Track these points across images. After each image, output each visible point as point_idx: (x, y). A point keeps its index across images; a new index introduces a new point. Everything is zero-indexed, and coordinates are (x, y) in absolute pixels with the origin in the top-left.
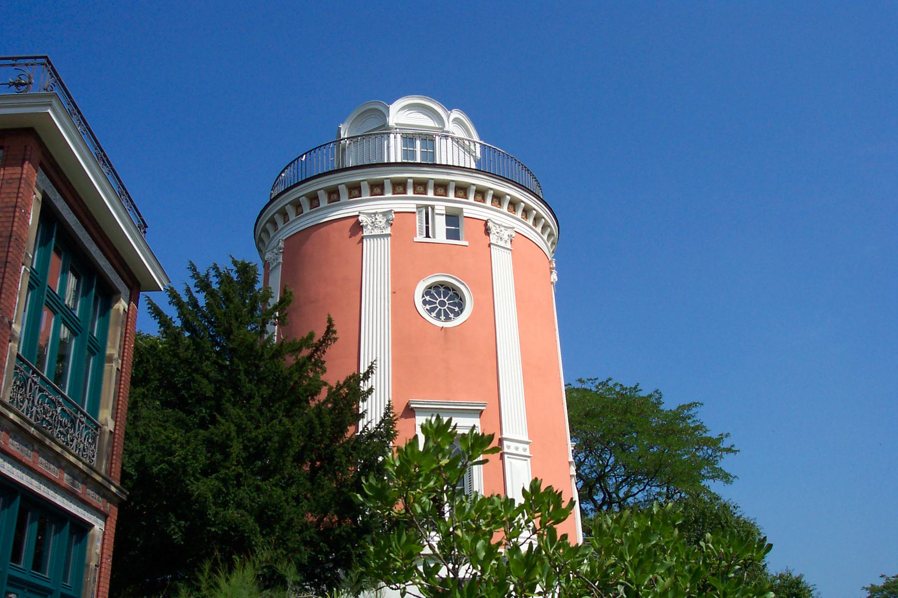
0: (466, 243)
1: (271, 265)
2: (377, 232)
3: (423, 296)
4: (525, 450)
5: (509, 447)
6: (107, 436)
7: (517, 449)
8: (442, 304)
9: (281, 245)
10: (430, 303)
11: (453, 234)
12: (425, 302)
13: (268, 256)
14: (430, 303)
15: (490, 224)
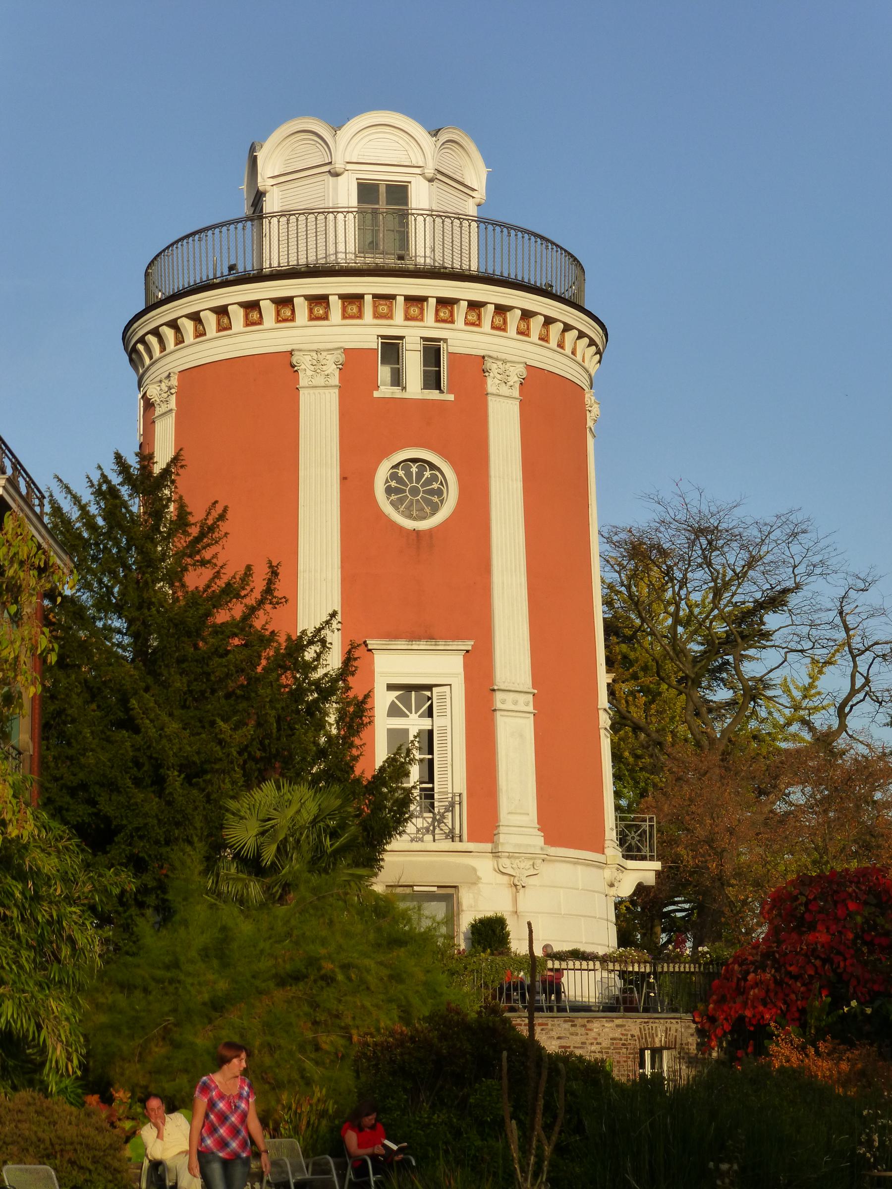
0: (451, 397)
1: (157, 409)
2: (320, 380)
3: (387, 482)
4: (527, 704)
5: (503, 702)
6: (28, 761)
7: (515, 703)
8: (414, 491)
9: (174, 381)
10: (397, 491)
11: (433, 380)
12: (389, 491)
13: (153, 392)
14: (397, 491)
15: (489, 364)
